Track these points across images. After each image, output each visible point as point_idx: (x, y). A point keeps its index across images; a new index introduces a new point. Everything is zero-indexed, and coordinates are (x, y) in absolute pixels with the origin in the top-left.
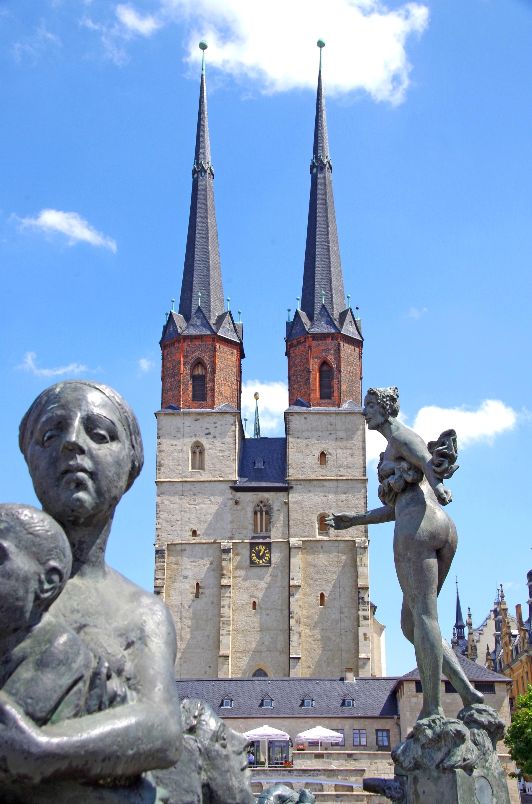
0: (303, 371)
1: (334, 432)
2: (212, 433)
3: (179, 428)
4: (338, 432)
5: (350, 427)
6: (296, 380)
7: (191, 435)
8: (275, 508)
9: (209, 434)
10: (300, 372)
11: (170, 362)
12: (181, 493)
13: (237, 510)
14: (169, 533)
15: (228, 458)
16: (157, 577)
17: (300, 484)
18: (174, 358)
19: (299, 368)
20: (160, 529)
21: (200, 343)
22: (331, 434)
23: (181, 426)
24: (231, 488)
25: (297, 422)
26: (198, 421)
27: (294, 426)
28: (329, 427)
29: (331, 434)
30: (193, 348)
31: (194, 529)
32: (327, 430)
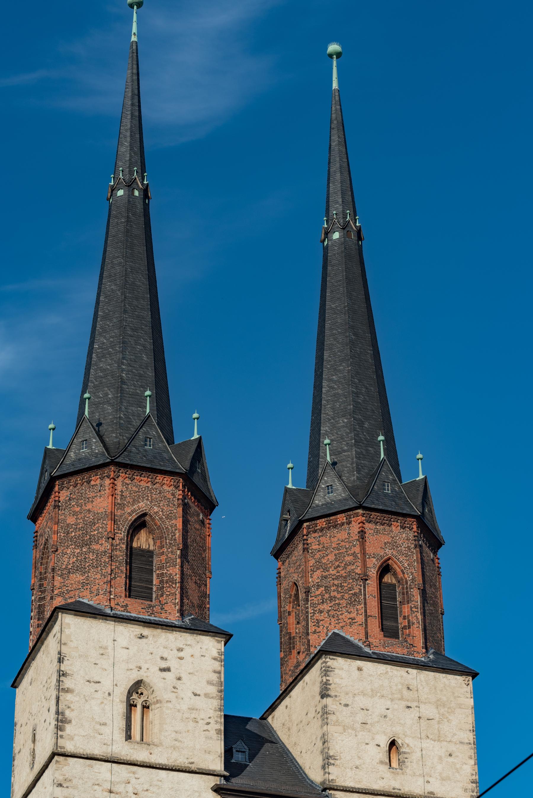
0: (345, 577)
2: (172, 669)
3: (106, 648)
5: (444, 699)
9: (168, 670)
10: (337, 578)
11: (75, 514)
12: (107, 786)
15: (206, 727)
18: (89, 506)
19: (335, 572)
21: (149, 484)
22: (408, 707)
23: (110, 644)
25: (343, 674)
26: (144, 640)
27: (337, 680)
28: (405, 692)
29: (408, 707)
30: (135, 492)
32: (402, 699)
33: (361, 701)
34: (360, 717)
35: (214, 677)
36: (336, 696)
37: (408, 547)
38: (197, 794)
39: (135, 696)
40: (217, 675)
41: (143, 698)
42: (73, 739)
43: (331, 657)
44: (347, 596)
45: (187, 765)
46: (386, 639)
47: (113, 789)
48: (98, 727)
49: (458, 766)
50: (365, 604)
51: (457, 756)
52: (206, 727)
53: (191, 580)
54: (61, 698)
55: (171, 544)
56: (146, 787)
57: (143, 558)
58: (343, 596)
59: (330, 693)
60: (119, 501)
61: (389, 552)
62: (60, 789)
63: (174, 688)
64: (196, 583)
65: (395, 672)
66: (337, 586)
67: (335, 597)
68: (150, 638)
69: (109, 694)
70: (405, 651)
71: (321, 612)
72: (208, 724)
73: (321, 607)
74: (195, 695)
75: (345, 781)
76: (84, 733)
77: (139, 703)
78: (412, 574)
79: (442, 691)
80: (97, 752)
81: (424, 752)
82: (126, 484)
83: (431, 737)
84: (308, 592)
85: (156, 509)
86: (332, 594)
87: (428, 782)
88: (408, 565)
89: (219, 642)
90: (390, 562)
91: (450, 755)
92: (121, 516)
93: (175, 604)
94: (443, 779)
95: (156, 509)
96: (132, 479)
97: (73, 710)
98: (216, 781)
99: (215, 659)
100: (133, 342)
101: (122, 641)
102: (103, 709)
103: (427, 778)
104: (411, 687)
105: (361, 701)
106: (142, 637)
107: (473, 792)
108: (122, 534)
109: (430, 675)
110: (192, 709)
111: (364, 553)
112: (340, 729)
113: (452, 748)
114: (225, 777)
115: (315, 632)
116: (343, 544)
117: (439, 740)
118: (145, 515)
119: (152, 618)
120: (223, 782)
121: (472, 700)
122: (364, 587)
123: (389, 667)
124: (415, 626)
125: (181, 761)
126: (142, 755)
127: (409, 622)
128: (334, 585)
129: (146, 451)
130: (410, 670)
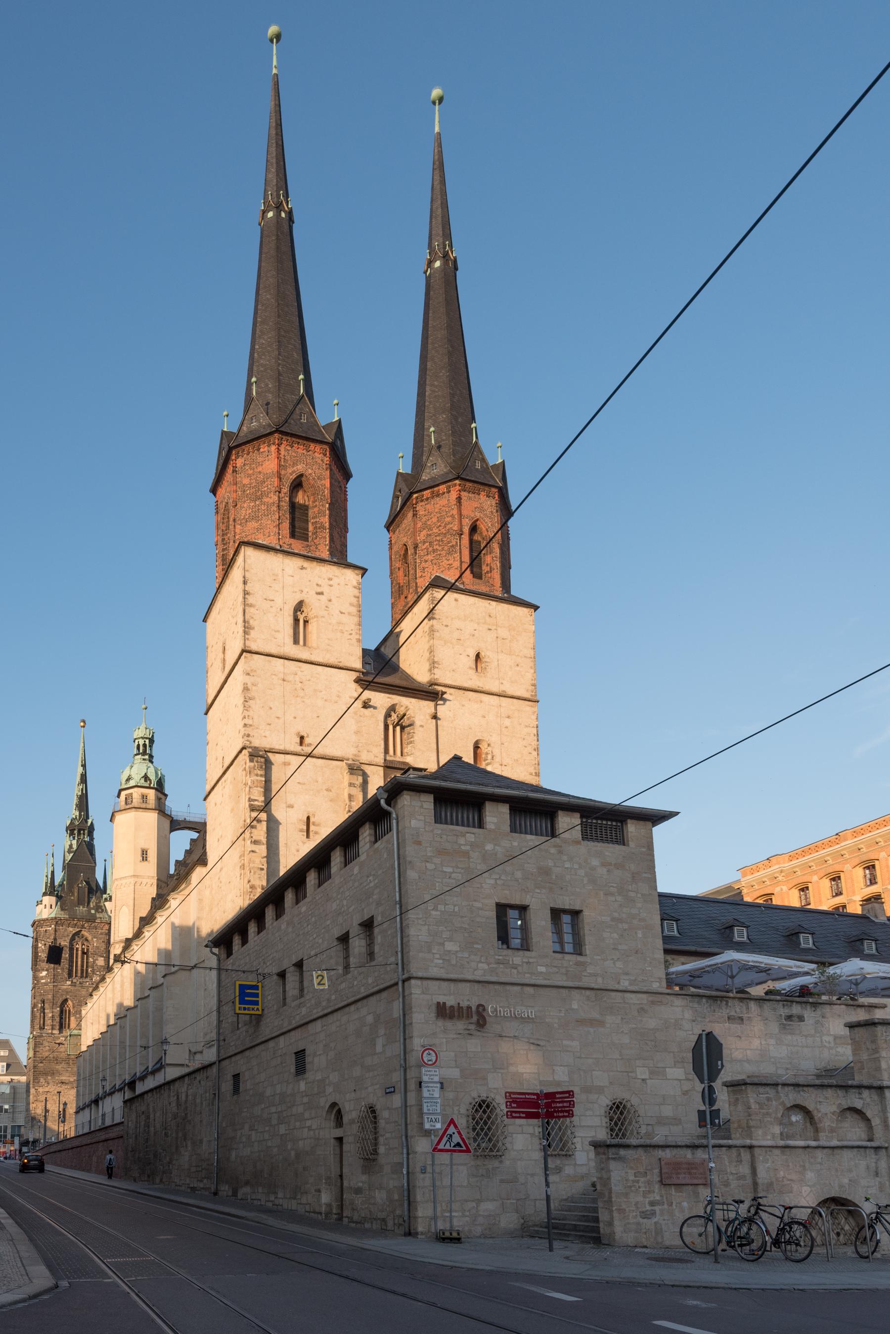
6: (431, 549)
9: (321, 593)
12: (281, 676)
14: (264, 735)
16: (252, 797)
20: (251, 725)
35: (355, 601)
39: (299, 613)
41: (304, 615)
44: (446, 548)
46: (474, 579)
50: (460, 552)
58: (443, 548)
62: (248, 676)
63: (327, 607)
66: (439, 541)
67: (437, 549)
69: (281, 609)
71: (426, 561)
72: (351, 634)
73: (426, 558)
74: (342, 613)
80: (273, 651)
84: (416, 547)
89: (357, 575)
99: (355, 587)
110: (339, 623)
111: (461, 515)
115: (421, 577)
120: (362, 676)
122: (460, 540)
126: (304, 655)
127: (491, 567)
128: (436, 540)
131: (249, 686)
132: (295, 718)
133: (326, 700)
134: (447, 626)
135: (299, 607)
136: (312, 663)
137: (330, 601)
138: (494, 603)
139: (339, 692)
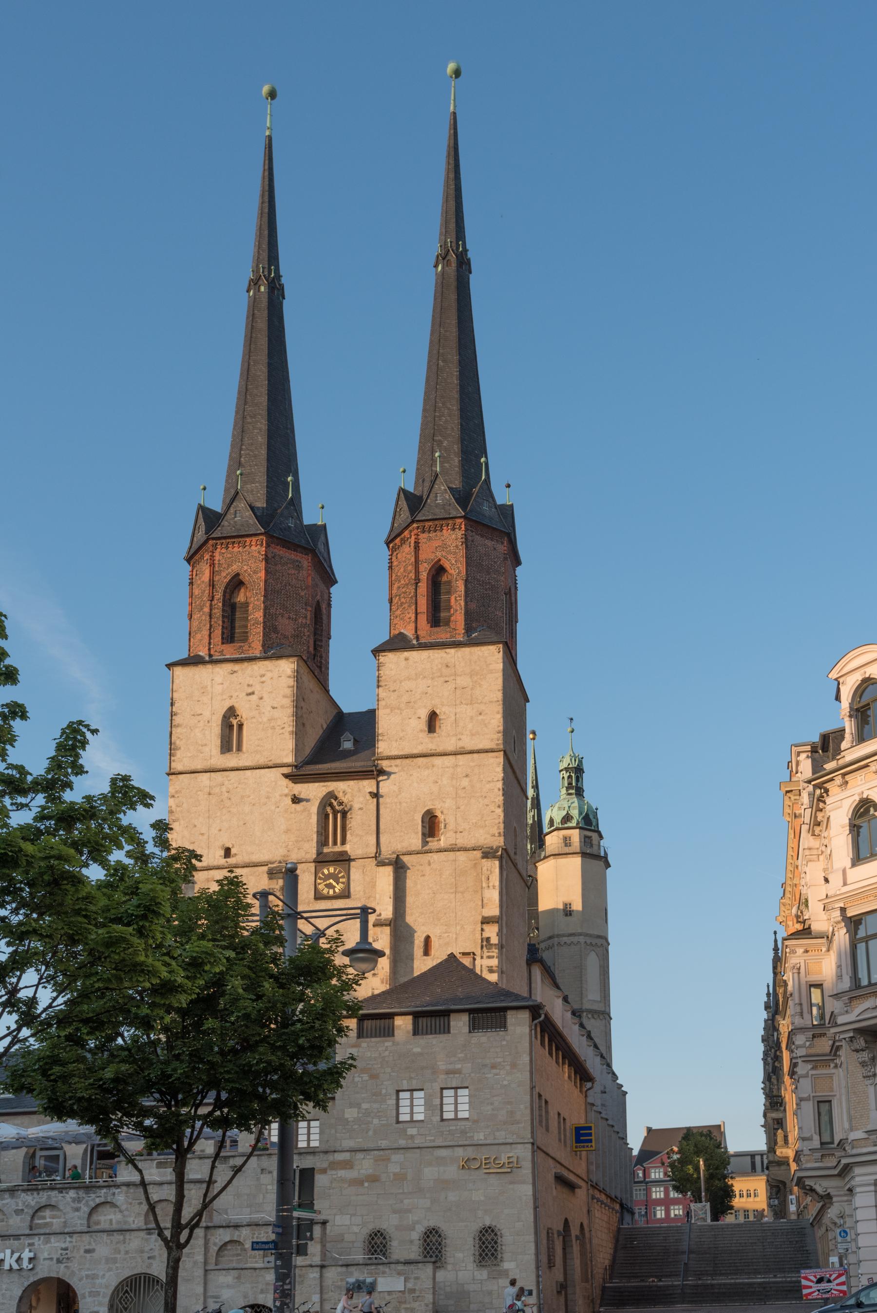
0: (407, 584)
1: (453, 678)
2: (256, 693)
4: (458, 678)
5: (478, 668)
7: (224, 697)
8: (356, 806)
9: (253, 693)
12: (207, 790)
13: (296, 811)
15: (281, 731)
17: (396, 766)
19: (402, 582)
21: (241, 549)
22: (446, 682)
23: (209, 683)
24: (286, 776)
26: (235, 675)
28: (445, 671)
29: (446, 682)
31: (227, 845)
32: (441, 676)
33: (407, 685)
34: (405, 698)
35: (289, 692)
36: (386, 685)
37: (457, 546)
38: (274, 783)
40: (291, 689)
42: (182, 761)
43: (383, 654)
44: (408, 599)
45: (266, 763)
47: (212, 792)
48: (200, 748)
49: (486, 722)
51: (487, 714)
52: (281, 731)
53: (282, 616)
54: (173, 732)
55: (256, 593)
56: (235, 785)
57: (243, 609)
59: (380, 684)
60: (217, 569)
61: (439, 554)
62: (173, 799)
64: (289, 618)
65: (436, 655)
66: (404, 593)
68: (240, 672)
69: (208, 722)
70: (448, 635)
72: (283, 728)
74: (274, 708)
75: (390, 751)
76: (189, 755)
77: (235, 722)
78: (458, 568)
79: (475, 662)
80: (199, 767)
81: (457, 716)
82: (223, 553)
83: (464, 703)
85: (245, 567)
86: (403, 600)
87: (460, 739)
88: (456, 561)
89: (292, 663)
90: (441, 563)
91: (480, 714)
92: (218, 581)
93: (259, 641)
94: (472, 735)
95: (245, 567)
96: (227, 548)
97: (182, 740)
98: (286, 770)
99: (289, 677)
100: (251, 427)
101: (218, 679)
102: (204, 734)
103: (459, 737)
104: (449, 665)
105: (407, 685)
106: (234, 672)
107: (498, 740)
108: (219, 595)
109: (467, 650)
112: (388, 711)
113: (482, 707)
114: (296, 766)
116: (408, 556)
117: (471, 704)
118: (238, 575)
119: (240, 656)
121: (502, 664)
123: (431, 651)
124: (458, 612)
125: (262, 761)
129: (235, 522)
130: (448, 650)
131: (174, 808)
132: (220, 830)
133: (254, 805)
134: (394, 691)
135: (231, 712)
136: (238, 769)
137: (261, 698)
138: (452, 651)
139: (268, 792)
